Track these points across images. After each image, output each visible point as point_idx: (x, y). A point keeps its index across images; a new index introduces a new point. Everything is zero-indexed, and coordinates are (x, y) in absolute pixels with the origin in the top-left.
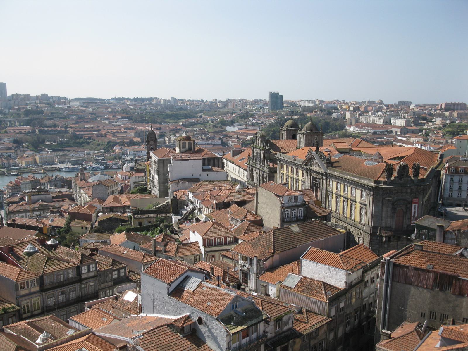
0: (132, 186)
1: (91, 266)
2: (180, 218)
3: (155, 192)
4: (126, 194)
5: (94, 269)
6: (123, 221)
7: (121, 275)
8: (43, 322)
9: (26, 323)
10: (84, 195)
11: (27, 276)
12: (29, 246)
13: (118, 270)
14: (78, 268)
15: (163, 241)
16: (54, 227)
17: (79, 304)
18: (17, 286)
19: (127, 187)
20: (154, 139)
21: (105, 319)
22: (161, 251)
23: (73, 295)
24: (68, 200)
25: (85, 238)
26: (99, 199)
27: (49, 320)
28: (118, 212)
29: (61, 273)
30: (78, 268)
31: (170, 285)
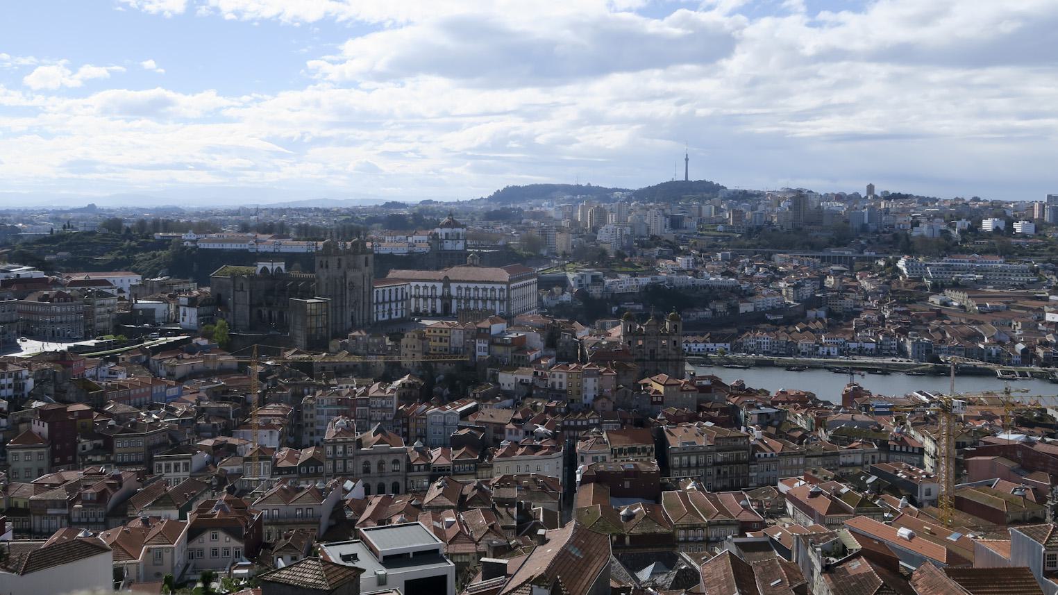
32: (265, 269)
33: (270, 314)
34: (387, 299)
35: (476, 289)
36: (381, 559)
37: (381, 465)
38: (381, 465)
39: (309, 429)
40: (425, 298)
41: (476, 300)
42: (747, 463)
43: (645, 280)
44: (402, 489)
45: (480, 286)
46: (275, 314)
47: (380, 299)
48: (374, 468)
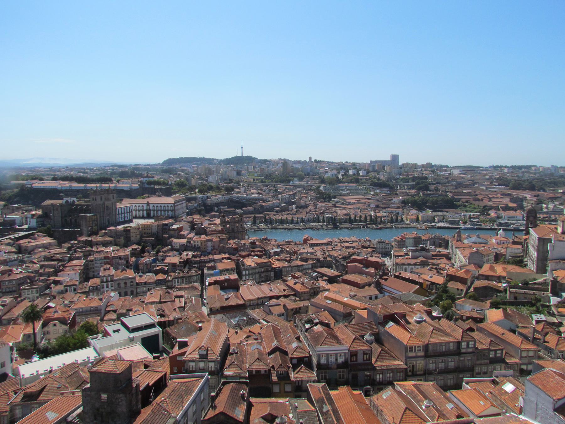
0: (508, 257)
1: (470, 343)
2: (559, 299)
3: (532, 266)
4: (502, 264)
5: (473, 346)
6: (500, 292)
7: (498, 355)
8: (425, 387)
9: (413, 385)
10: (460, 255)
11: (415, 342)
12: (418, 315)
13: (495, 351)
14: (459, 343)
15: (542, 330)
16: (433, 283)
17: (456, 374)
18: (408, 349)
19: (502, 255)
20: (534, 215)
21: (482, 403)
22: (540, 339)
23: (452, 365)
24: (445, 259)
25: (461, 303)
26: (475, 264)
27: (432, 387)
28: (493, 281)
29: (444, 344)
30: (459, 343)
31: (556, 402)
32: (67, 202)
33: (71, 220)
34: (123, 212)
35: (161, 206)
36: (131, 330)
37: (126, 283)
38: (126, 283)
39: (92, 270)
40: (139, 211)
41: (161, 211)
42: (270, 271)
43: (228, 197)
44: (135, 293)
45: (162, 205)
46: (73, 221)
47: (120, 212)
48: (122, 285)
